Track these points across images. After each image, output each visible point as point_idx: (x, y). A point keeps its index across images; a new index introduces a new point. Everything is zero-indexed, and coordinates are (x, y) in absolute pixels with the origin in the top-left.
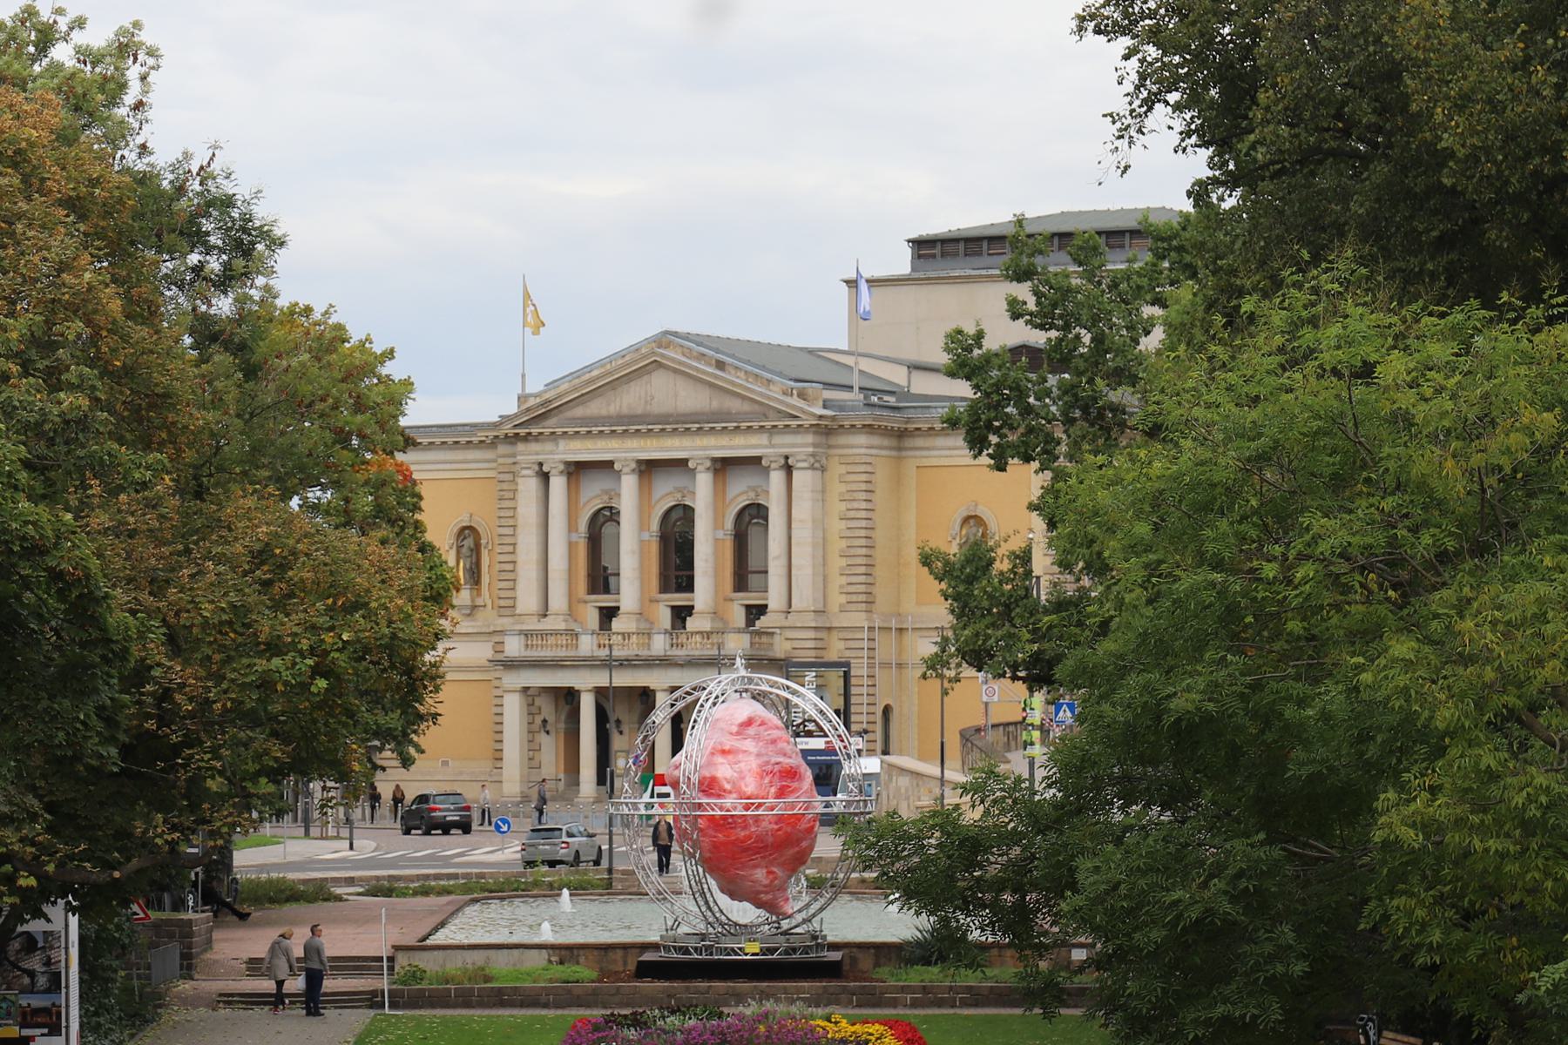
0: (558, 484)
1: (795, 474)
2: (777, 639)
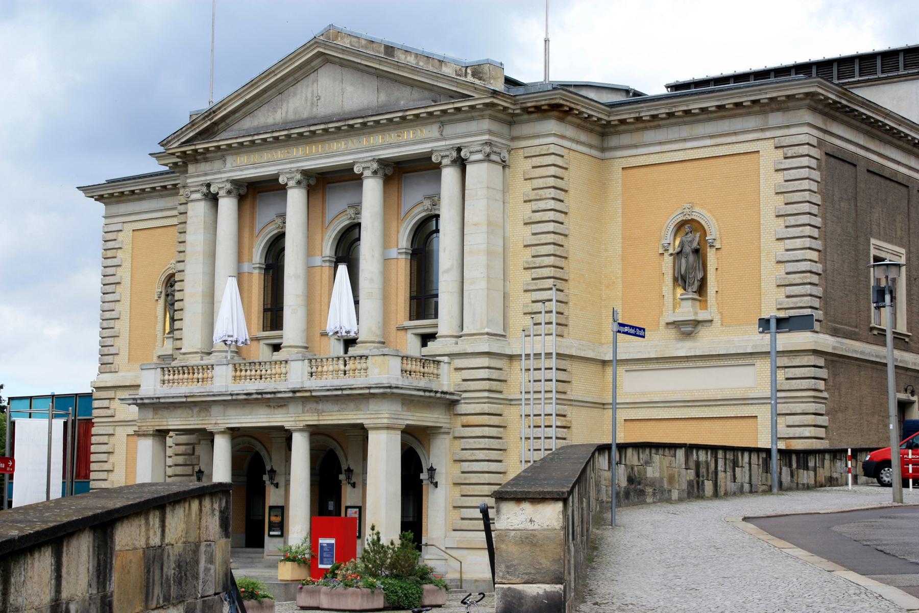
0: (228, 205)
1: (469, 168)
2: (444, 369)
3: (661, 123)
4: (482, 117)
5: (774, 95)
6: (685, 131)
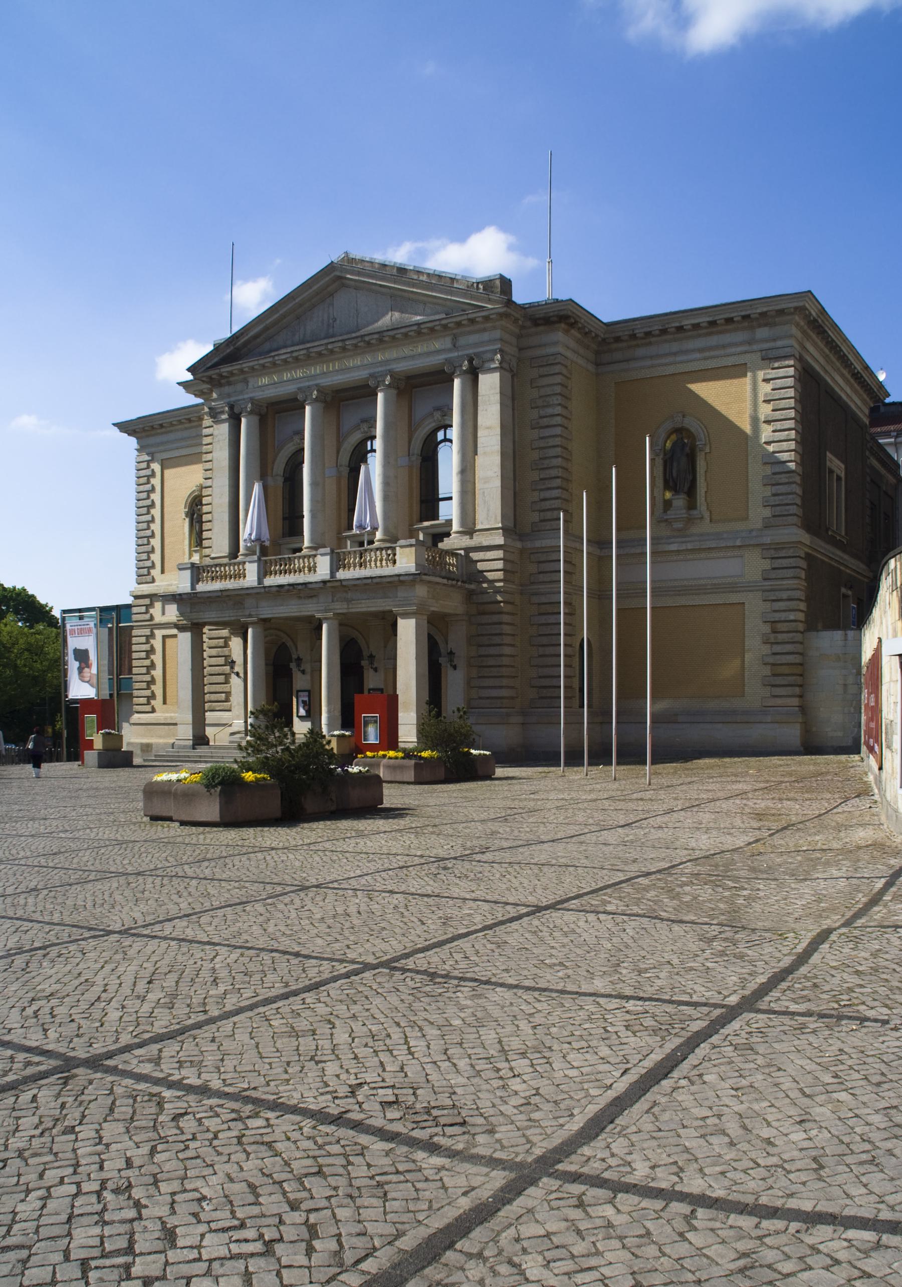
1: (481, 377)
3: (653, 339)
4: (495, 328)
5: (765, 309)
6: (675, 347)
